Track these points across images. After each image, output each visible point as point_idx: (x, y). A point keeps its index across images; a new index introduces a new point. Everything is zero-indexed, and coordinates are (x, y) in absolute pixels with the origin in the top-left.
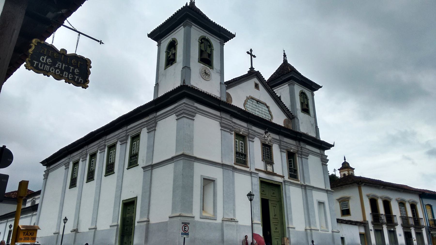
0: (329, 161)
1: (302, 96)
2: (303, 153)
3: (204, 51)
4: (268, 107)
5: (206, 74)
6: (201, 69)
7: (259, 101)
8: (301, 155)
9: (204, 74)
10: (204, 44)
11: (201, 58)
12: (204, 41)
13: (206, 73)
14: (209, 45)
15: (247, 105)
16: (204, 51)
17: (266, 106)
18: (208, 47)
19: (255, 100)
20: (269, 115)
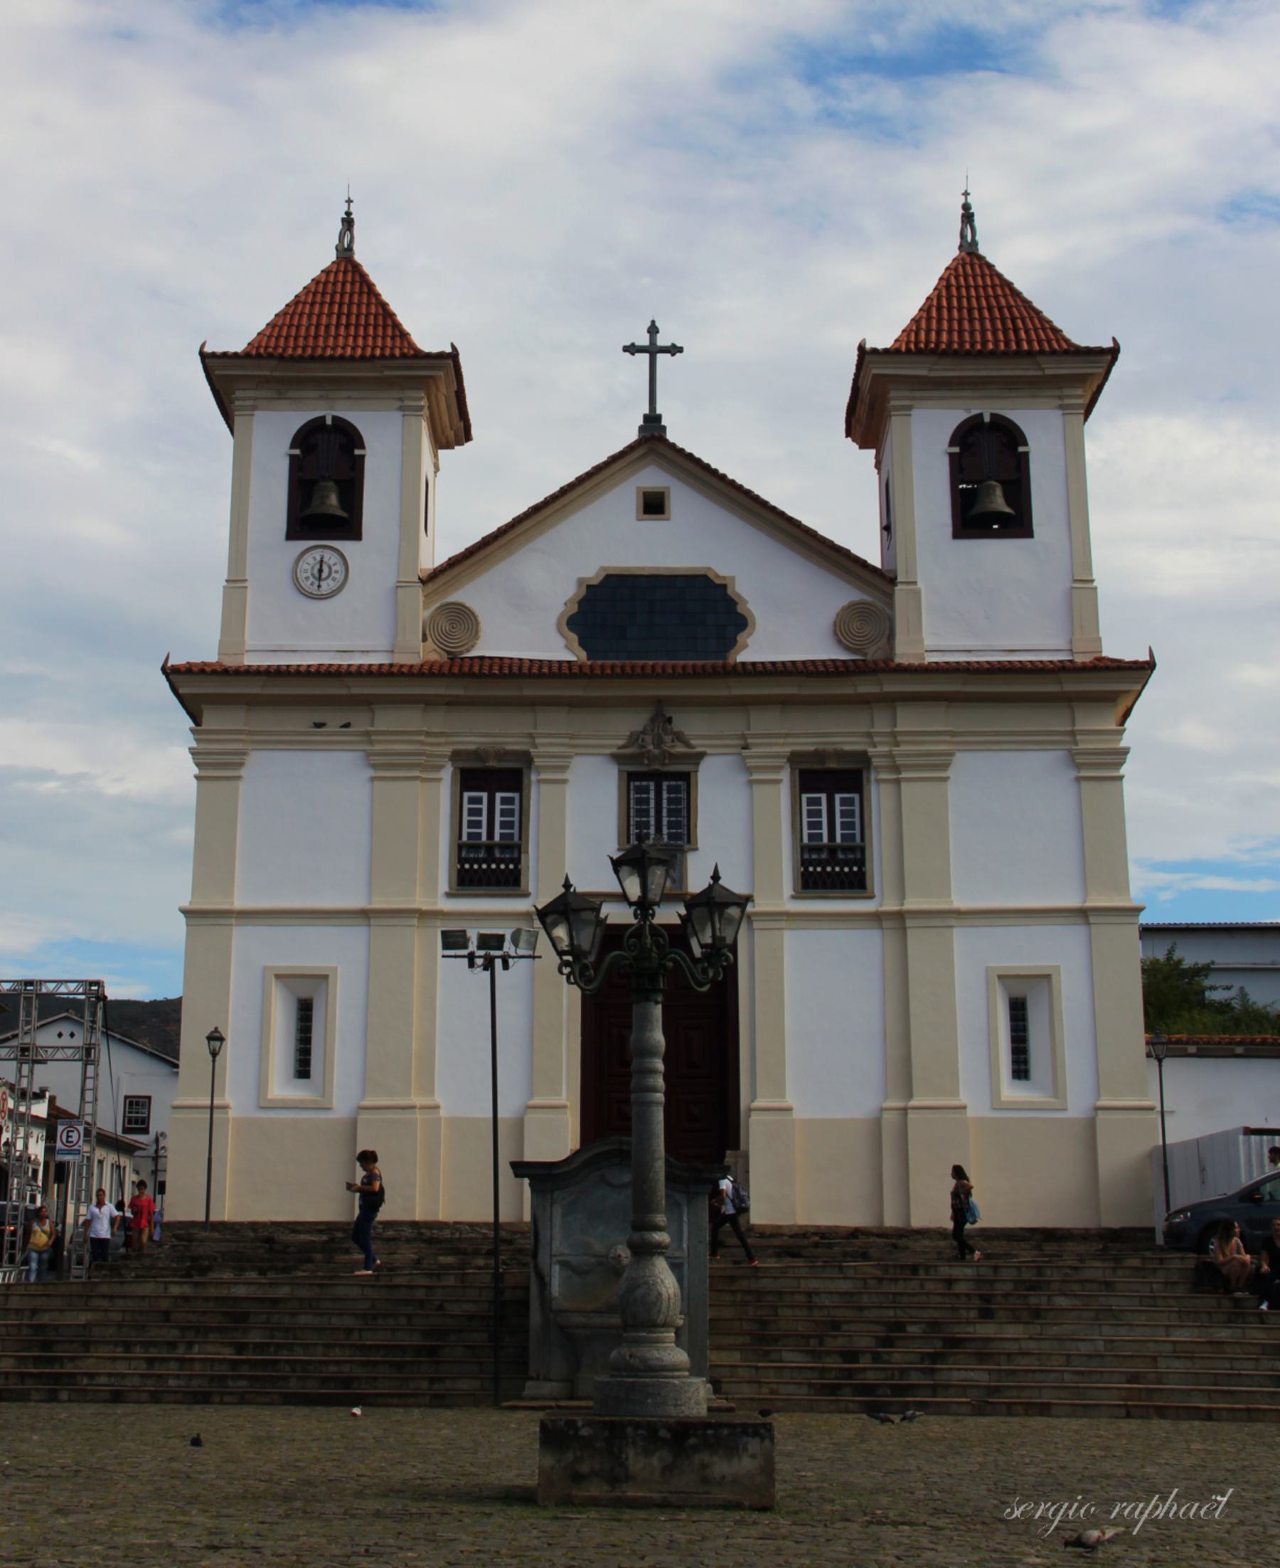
0: (1129, 756)
2: (899, 761)
8: (896, 769)
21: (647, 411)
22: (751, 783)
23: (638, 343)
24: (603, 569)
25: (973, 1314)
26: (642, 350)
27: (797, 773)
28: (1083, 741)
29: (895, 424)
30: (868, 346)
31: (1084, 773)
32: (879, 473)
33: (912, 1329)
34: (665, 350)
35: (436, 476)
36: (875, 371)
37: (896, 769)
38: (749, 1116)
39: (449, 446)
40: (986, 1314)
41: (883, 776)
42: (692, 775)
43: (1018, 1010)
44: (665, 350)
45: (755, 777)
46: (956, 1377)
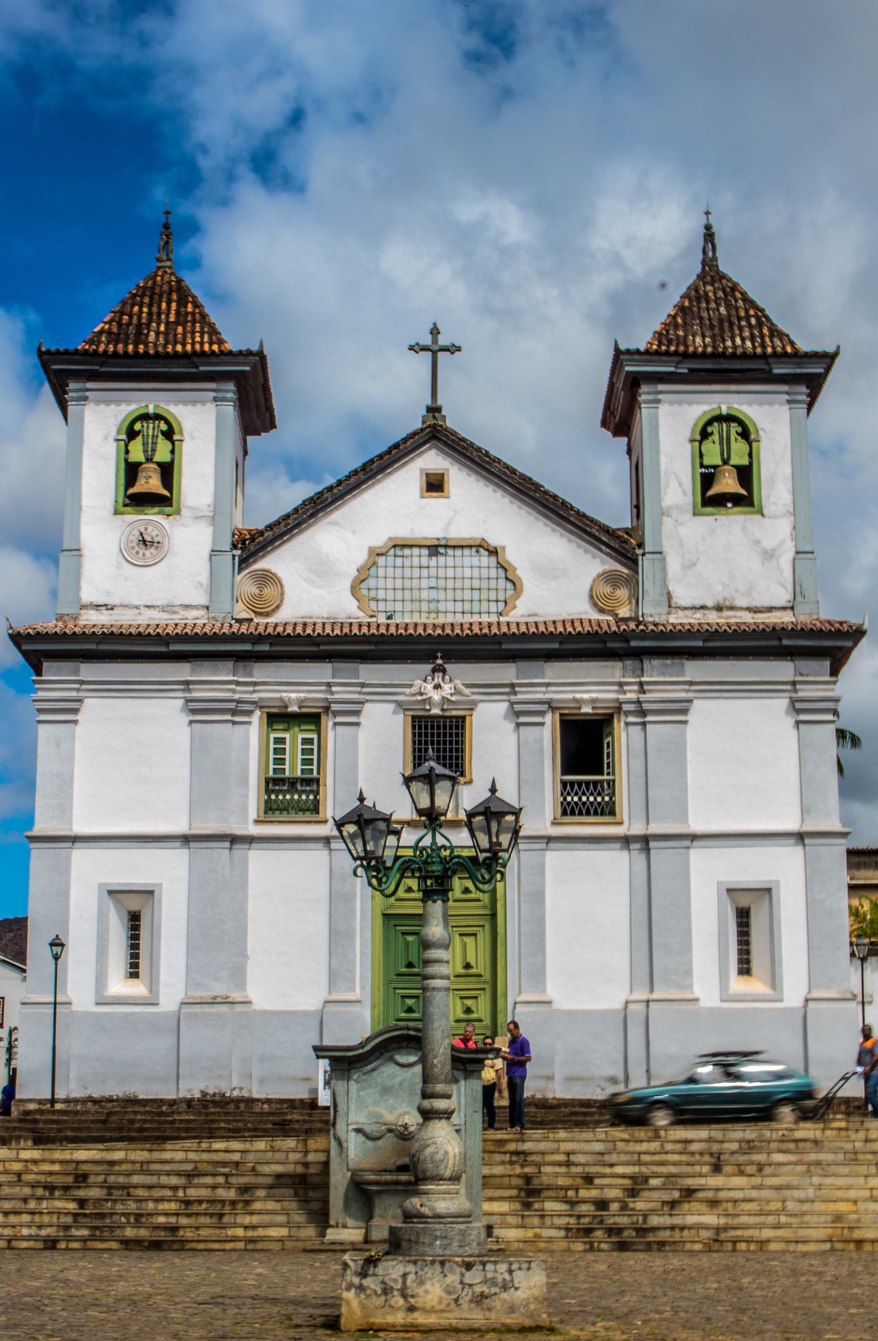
1: (716, 437)
3: (143, 459)
4: (493, 552)
5: (146, 545)
6: (126, 534)
7: (443, 543)
9: (137, 549)
10: (143, 435)
11: (131, 491)
12: (143, 426)
13: (144, 542)
14: (163, 433)
15: (371, 583)
16: (140, 464)
17: (487, 550)
18: (160, 435)
19: (420, 546)
20: (502, 583)
21: (429, 403)
22: (518, 725)
23: (422, 343)
24: (391, 539)
25: (706, 1169)
26: (425, 349)
27: (557, 716)
28: (801, 690)
29: (645, 413)
30: (623, 347)
31: (803, 717)
32: (630, 459)
33: (653, 1182)
34: (445, 349)
35: (244, 459)
36: (627, 369)
37: (643, 713)
38: (515, 1008)
39: (257, 433)
40: (717, 1168)
41: (631, 719)
42: (468, 718)
43: (743, 916)
44: (445, 349)
45: (522, 719)
46: (691, 1220)
